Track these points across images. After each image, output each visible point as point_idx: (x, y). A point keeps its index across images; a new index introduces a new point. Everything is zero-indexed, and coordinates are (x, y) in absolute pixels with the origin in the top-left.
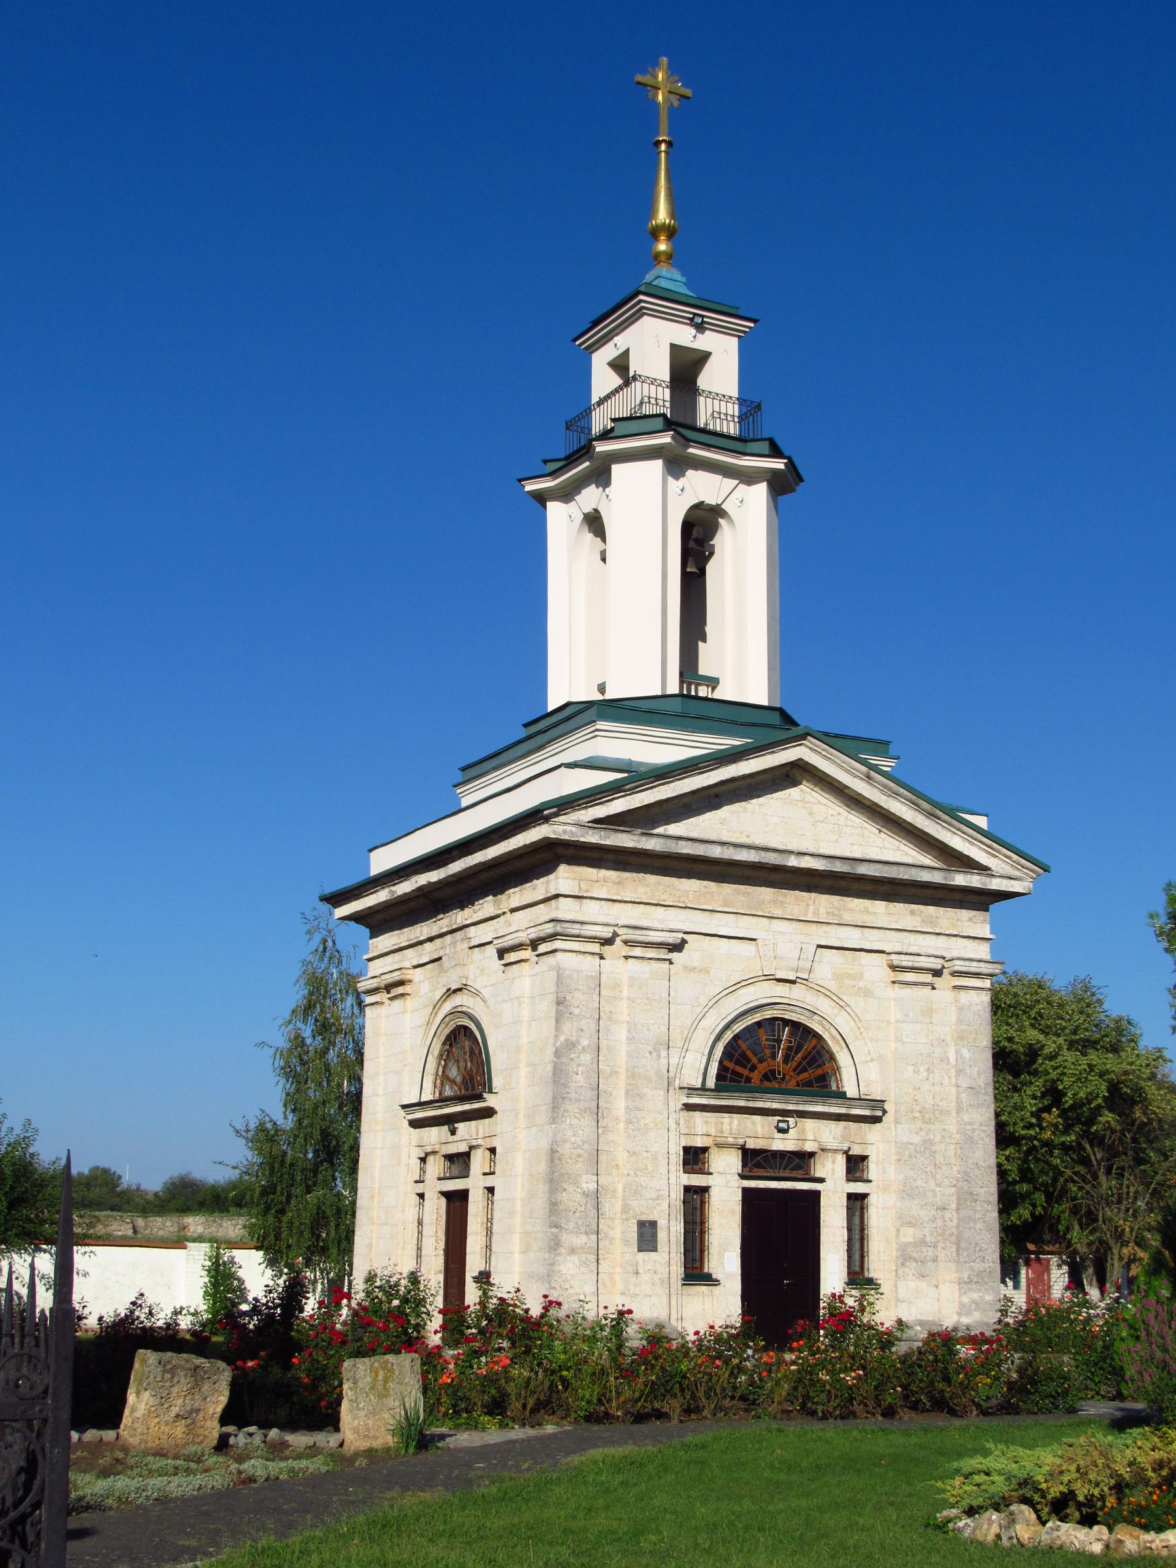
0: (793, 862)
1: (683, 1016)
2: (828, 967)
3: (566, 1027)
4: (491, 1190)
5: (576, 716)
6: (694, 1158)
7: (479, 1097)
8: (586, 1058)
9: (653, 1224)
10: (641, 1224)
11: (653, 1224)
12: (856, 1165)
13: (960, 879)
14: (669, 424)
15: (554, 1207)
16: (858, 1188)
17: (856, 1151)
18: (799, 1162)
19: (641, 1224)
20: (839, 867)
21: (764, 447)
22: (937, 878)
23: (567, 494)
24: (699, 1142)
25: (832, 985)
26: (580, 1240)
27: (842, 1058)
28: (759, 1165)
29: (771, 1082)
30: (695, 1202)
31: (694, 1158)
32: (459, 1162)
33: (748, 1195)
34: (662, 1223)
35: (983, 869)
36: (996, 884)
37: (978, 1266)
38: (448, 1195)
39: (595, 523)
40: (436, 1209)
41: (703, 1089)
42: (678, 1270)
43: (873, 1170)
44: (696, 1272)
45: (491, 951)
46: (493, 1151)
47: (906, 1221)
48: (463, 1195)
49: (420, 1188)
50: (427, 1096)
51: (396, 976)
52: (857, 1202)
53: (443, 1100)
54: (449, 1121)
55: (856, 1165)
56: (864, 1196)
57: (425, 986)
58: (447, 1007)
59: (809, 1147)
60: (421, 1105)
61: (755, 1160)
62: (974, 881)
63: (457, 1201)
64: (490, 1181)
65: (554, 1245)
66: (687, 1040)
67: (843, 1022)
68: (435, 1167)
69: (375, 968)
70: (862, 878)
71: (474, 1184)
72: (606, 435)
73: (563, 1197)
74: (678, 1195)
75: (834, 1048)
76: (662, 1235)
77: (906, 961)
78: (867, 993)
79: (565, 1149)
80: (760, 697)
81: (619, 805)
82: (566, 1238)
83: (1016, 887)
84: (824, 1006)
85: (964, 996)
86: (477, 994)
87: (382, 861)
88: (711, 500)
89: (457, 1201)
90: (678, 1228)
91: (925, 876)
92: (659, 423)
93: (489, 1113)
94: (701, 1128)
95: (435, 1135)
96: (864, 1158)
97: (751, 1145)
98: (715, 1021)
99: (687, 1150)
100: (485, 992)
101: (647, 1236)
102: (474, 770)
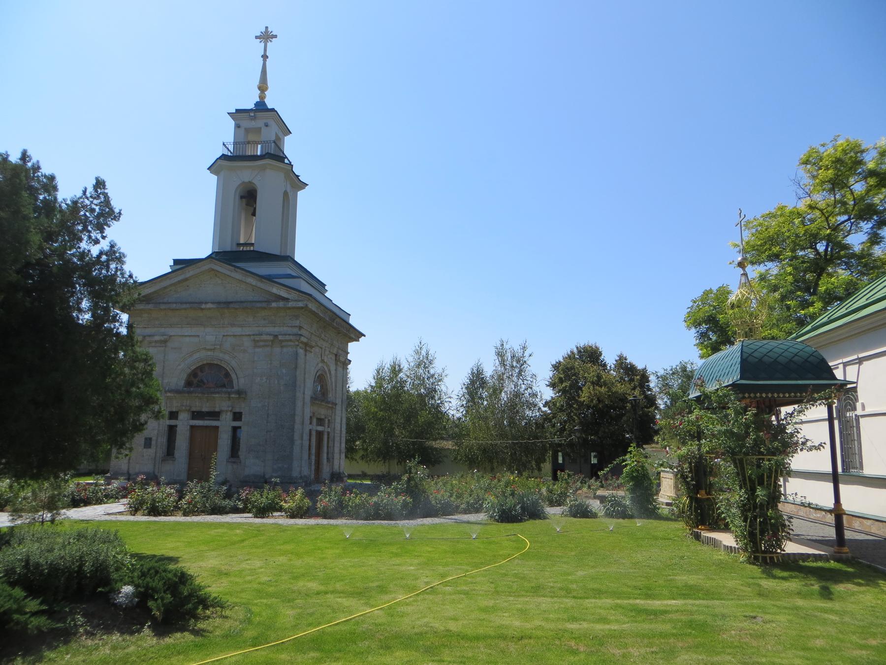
9: (150, 439)
10: (146, 439)
11: (150, 439)
12: (237, 416)
17: (237, 410)
18: (215, 415)
19: (146, 439)
34: (154, 438)
35: (286, 300)
41: (178, 392)
52: (235, 429)
55: (237, 416)
59: (217, 410)
76: (153, 443)
84: (227, 357)
85: (285, 350)
88: (247, 180)
96: (240, 414)
97: (194, 409)
101: (148, 443)
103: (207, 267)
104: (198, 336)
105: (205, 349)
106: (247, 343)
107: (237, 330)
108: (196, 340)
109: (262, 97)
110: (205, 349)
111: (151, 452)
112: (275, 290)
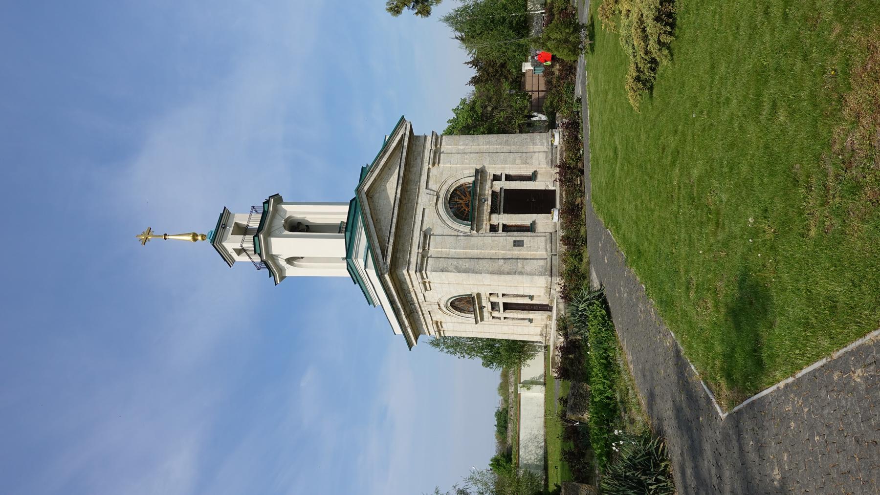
0: (398, 196)
1: (447, 231)
2: (433, 186)
3: (450, 269)
4: (503, 295)
5: (351, 269)
6: (493, 229)
7: (473, 298)
8: (461, 262)
9: (515, 241)
10: (514, 245)
11: (515, 241)
12: (496, 178)
13: (406, 144)
14: (257, 235)
15: (508, 273)
16: (503, 177)
17: (492, 178)
19: (514, 245)
20: (400, 181)
21: (266, 205)
22: (405, 151)
23: (281, 270)
24: (488, 227)
25: (439, 185)
26: (520, 265)
27: (462, 182)
28: (496, 208)
29: (470, 204)
30: (507, 228)
31: (493, 229)
32: (494, 306)
33: (506, 211)
34: (514, 239)
35: (403, 136)
36: (408, 133)
37: (529, 140)
38: (505, 309)
39: (290, 261)
40: (510, 314)
42: (529, 234)
43: (498, 173)
44: (530, 229)
45: (426, 294)
46: (491, 294)
47: (514, 163)
48: (504, 304)
49: (502, 319)
50: (473, 316)
51: (435, 325)
52: (509, 178)
53: (474, 311)
54: (481, 308)
55: (496, 178)
56: (506, 175)
57: (438, 316)
58: (445, 309)
59: (490, 192)
60: (476, 318)
61: (494, 210)
62: (406, 139)
63: (507, 307)
64: (500, 295)
65: (521, 273)
66: (455, 230)
67: (450, 182)
68: (495, 314)
69: (432, 333)
70: (404, 174)
71: (501, 300)
72: (260, 255)
73: (506, 270)
74: (505, 234)
75: (458, 184)
76: (518, 239)
77: (431, 161)
78: (442, 173)
79: (490, 269)
80: (346, 208)
81: (379, 251)
82: (519, 270)
83: (409, 126)
84: (445, 188)
86: (440, 299)
87: (398, 330)
89: (507, 307)
90: (516, 234)
91: (404, 154)
92: (256, 238)
93: (479, 295)
94: (486, 226)
95: (486, 314)
96: (494, 175)
97: (489, 210)
98: (449, 222)
99: (490, 231)
100: (440, 296)
101: (518, 244)
102: (370, 301)
103: (364, 197)
104: (424, 209)
105: (436, 204)
106: (434, 171)
107: (424, 178)
108: (426, 211)
109: (203, 236)
110: (436, 204)
111: (525, 239)
112: (394, 145)
